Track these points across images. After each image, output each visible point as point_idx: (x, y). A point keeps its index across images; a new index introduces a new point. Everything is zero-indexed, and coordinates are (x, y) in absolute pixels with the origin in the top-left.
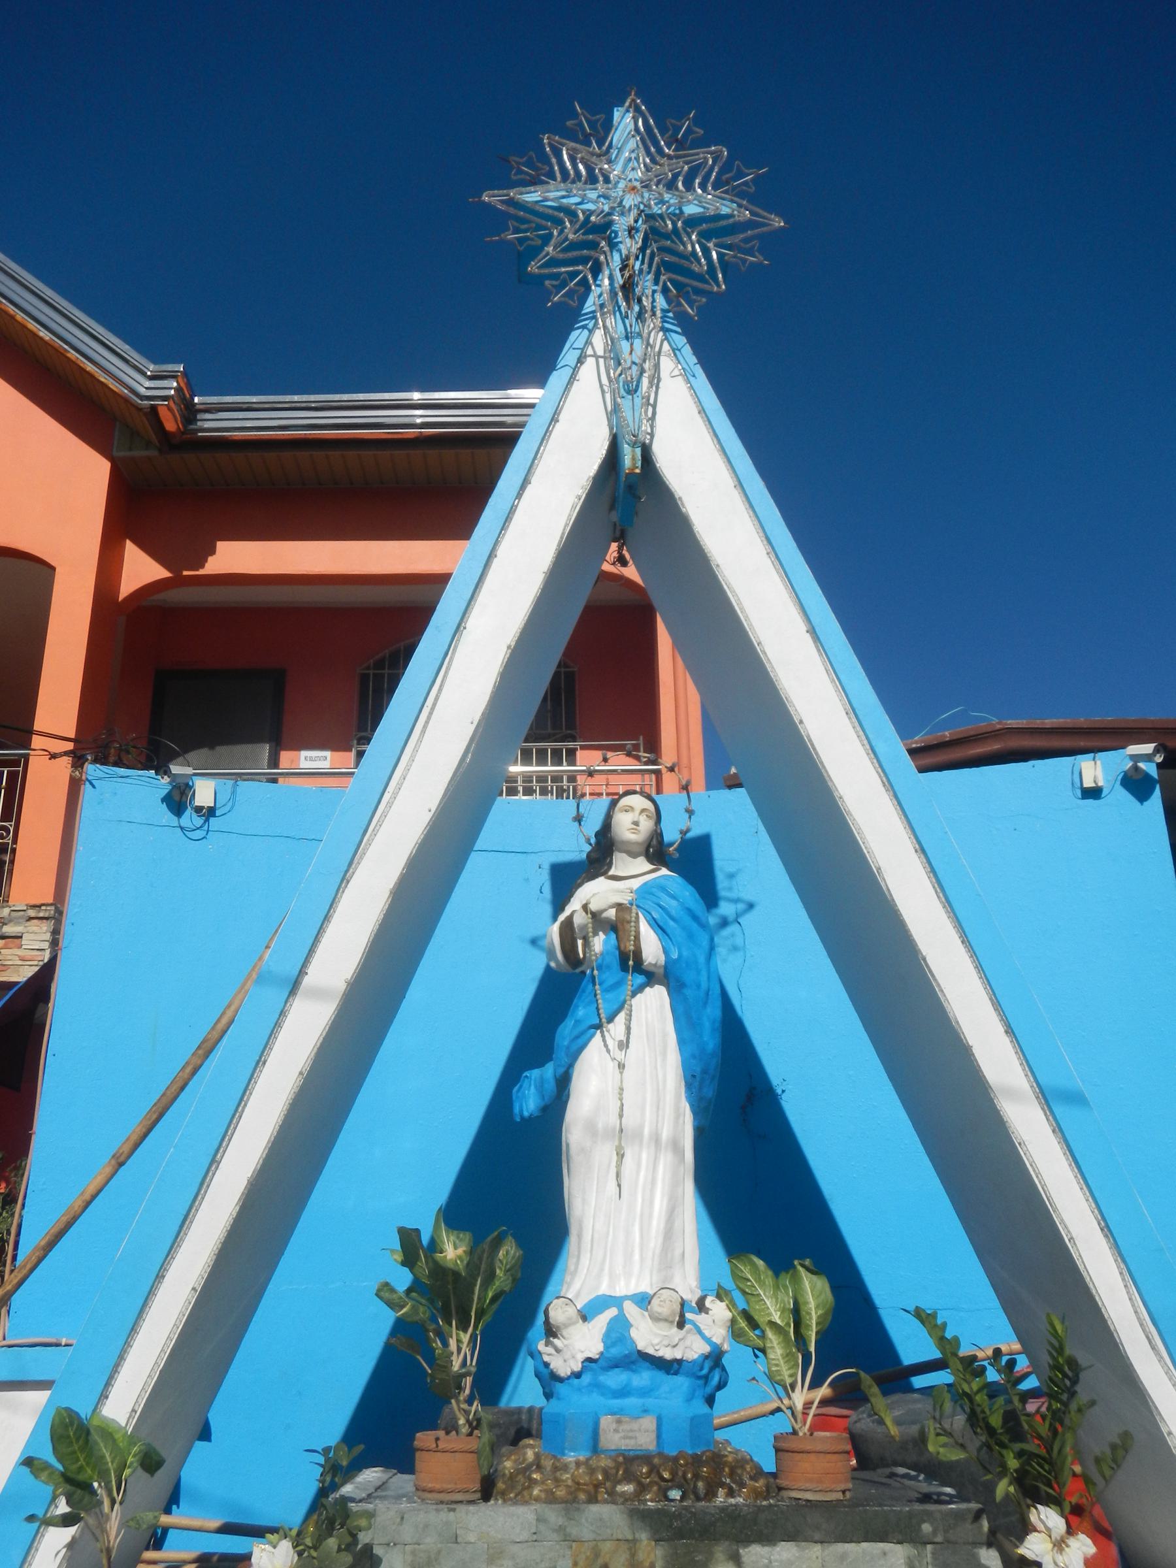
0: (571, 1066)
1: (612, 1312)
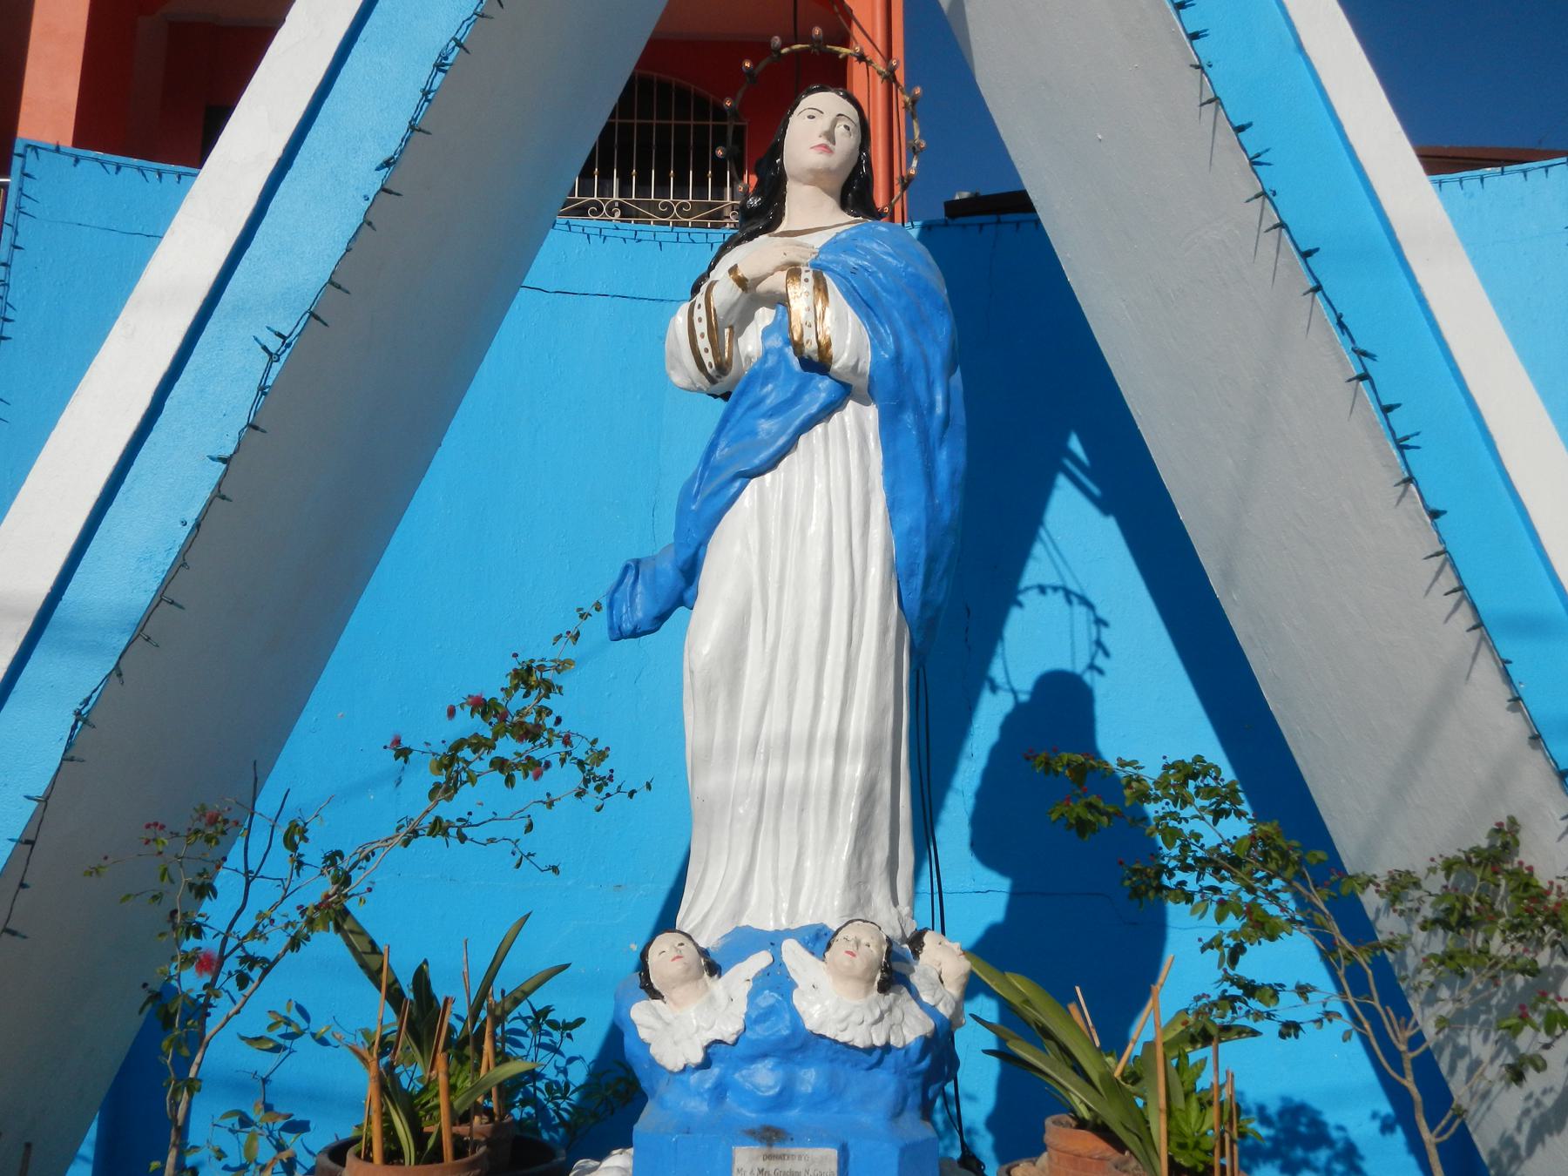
0: (703, 544)
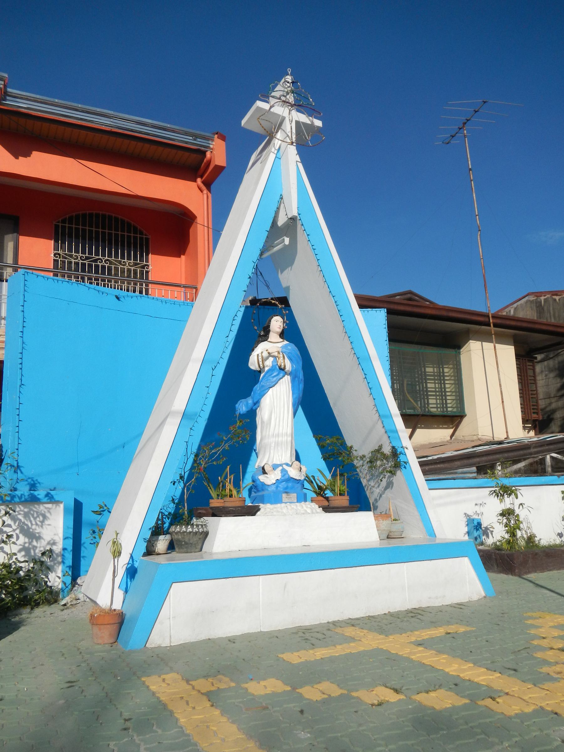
0: (261, 399)
1: (280, 468)
